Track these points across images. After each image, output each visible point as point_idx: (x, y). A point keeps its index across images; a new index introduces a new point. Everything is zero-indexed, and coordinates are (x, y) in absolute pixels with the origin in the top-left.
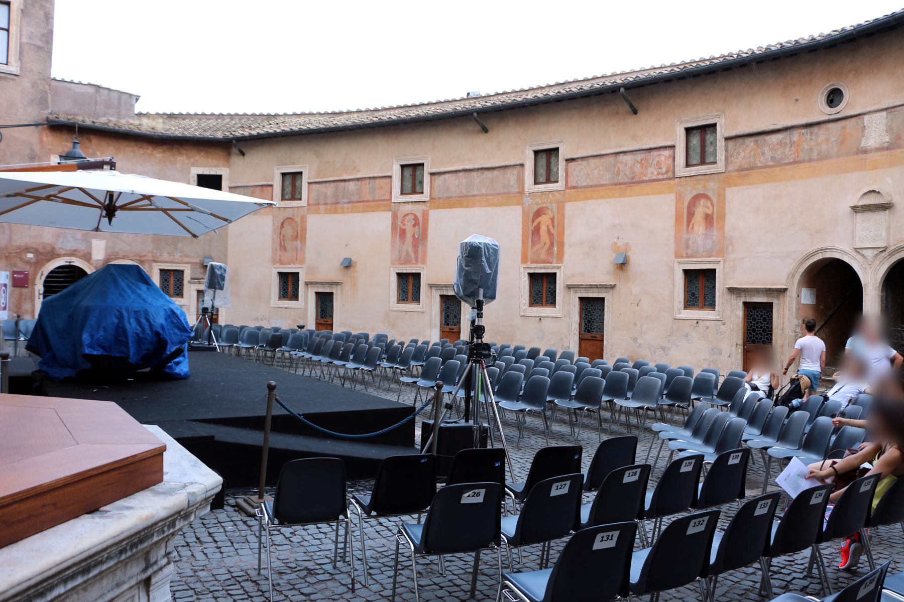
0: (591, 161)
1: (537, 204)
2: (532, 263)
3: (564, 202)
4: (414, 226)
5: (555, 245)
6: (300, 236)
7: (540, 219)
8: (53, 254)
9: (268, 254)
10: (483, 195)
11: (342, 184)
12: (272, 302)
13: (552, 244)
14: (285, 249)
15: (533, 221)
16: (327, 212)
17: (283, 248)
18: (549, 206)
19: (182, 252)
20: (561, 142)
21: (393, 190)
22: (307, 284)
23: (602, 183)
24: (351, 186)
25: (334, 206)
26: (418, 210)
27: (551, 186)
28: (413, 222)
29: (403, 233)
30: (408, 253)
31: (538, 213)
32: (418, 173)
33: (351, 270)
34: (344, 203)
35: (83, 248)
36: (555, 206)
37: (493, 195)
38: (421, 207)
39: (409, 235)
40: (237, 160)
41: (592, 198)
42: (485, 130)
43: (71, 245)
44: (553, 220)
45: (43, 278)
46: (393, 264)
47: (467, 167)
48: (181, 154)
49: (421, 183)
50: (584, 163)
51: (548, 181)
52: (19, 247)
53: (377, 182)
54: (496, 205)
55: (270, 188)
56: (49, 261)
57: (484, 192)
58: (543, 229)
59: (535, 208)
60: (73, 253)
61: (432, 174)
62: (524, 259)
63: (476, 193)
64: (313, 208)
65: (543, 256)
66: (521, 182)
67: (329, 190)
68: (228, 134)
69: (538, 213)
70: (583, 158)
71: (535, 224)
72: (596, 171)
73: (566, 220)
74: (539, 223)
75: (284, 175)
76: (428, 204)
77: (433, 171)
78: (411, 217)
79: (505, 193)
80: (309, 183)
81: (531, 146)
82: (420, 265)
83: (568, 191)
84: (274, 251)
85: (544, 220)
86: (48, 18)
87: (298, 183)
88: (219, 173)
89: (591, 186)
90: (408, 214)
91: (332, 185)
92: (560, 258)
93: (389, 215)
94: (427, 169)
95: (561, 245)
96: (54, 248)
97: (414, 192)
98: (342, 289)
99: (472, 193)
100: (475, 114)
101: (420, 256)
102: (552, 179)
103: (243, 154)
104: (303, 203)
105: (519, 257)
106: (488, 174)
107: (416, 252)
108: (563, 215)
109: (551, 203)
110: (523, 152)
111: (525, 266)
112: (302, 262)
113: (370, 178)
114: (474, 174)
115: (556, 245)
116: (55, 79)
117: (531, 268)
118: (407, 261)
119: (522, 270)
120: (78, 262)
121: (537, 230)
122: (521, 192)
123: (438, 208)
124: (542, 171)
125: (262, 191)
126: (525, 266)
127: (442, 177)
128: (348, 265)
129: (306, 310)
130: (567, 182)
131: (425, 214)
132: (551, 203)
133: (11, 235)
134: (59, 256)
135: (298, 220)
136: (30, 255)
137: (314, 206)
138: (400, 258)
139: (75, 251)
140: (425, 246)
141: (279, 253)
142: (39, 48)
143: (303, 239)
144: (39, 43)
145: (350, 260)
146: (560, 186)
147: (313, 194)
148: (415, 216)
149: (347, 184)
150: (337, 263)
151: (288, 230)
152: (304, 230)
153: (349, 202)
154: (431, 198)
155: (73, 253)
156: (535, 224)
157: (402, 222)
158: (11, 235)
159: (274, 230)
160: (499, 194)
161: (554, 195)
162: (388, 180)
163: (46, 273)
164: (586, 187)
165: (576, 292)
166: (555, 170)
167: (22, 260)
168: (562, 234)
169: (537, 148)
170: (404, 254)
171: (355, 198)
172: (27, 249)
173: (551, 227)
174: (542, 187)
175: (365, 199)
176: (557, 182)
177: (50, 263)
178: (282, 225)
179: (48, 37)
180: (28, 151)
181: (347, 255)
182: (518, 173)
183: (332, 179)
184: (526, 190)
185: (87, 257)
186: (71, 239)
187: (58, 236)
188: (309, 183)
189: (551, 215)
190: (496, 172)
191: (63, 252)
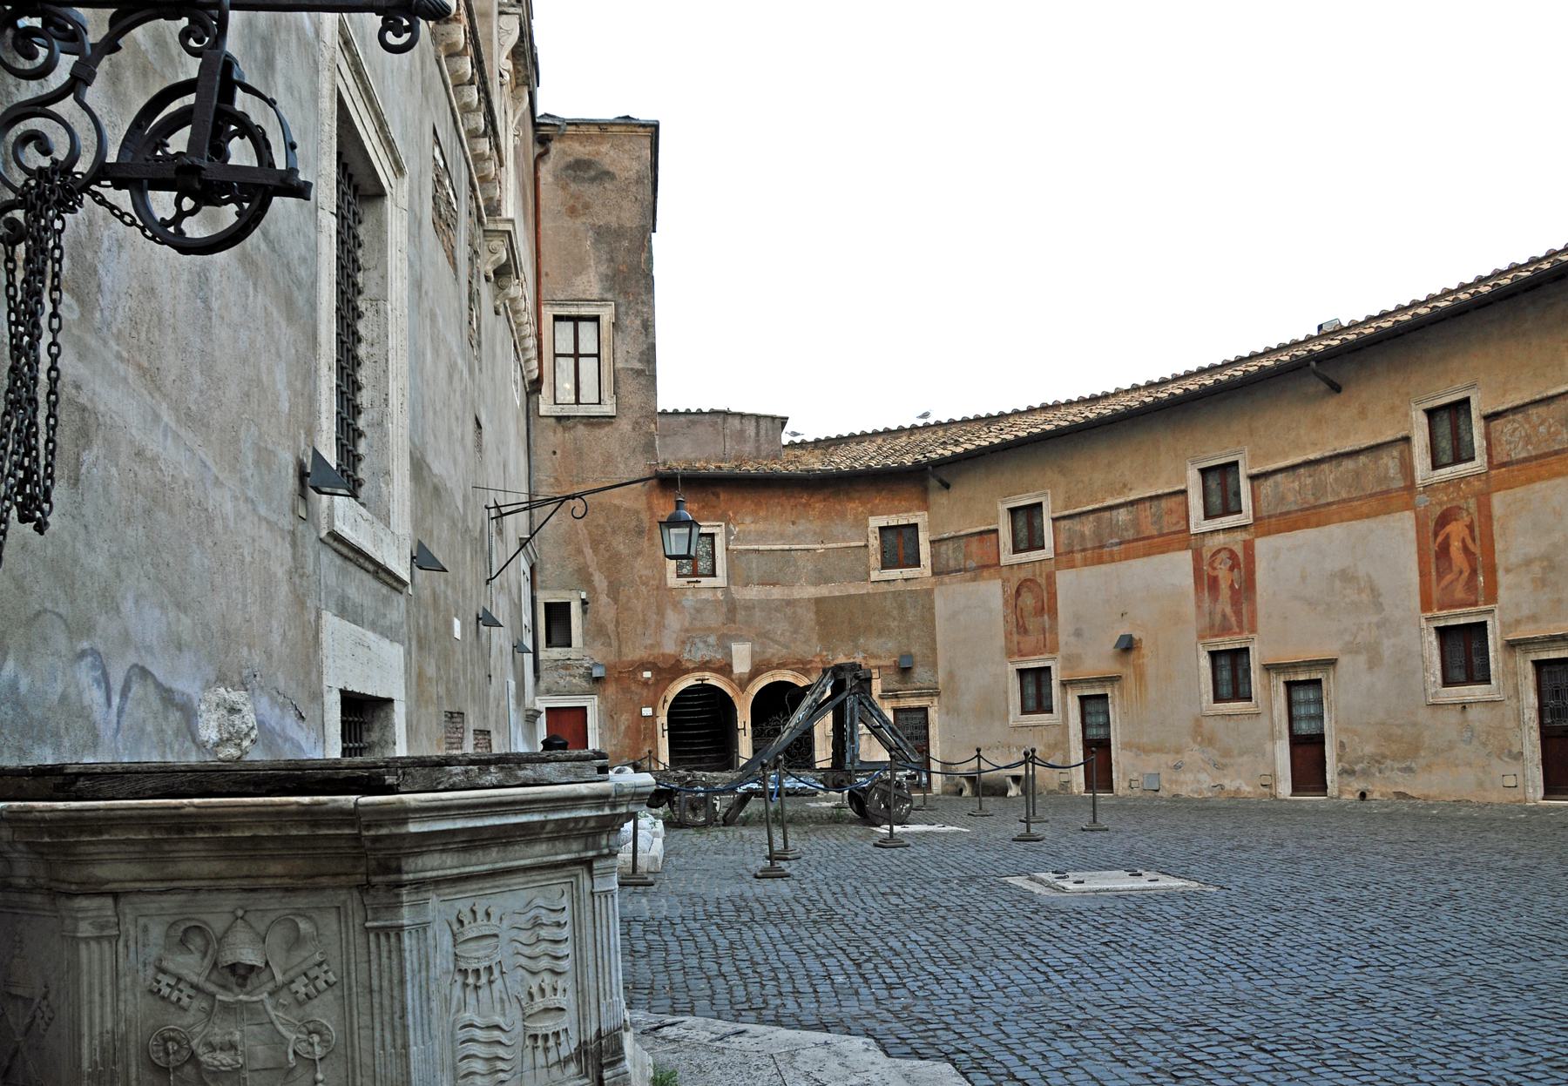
0: (1533, 411)
1: (1440, 504)
2: (1440, 609)
3: (1489, 494)
4: (1231, 569)
5: (1480, 571)
6: (1048, 607)
7: (1448, 529)
8: (676, 669)
9: (1000, 641)
10: (1344, 501)
11: (1107, 514)
12: (1011, 718)
13: (1474, 572)
14: (1026, 631)
15: (1436, 535)
16: (1085, 564)
17: (1022, 629)
18: (1462, 503)
19: (865, 651)
20: (1473, 386)
21: (1192, 514)
22: (1064, 684)
23: (1557, 447)
24: (1122, 515)
25: (1098, 554)
26: (1236, 541)
27: (1462, 469)
28: (1230, 563)
29: (1214, 583)
30: (1224, 616)
31: (1444, 519)
32: (1230, 479)
33: (1133, 655)
34: (1113, 545)
36: (1472, 503)
37: (1360, 498)
38: (1241, 536)
39: (1224, 586)
40: (940, 499)
41: (1540, 478)
42: (1336, 388)
43: (701, 653)
44: (1471, 527)
45: (667, 706)
46: (1201, 637)
47: (1312, 457)
48: (851, 499)
49: (1237, 494)
50: (1519, 417)
51: (1457, 460)
52: (632, 663)
53: (1164, 504)
54: (1368, 517)
55: (993, 536)
57: (1344, 495)
58: (1455, 545)
59: (1438, 511)
60: (704, 666)
61: (1253, 478)
62: (1426, 605)
63: (1330, 499)
64: (1064, 559)
65: (1459, 594)
66: (1407, 468)
67: (1087, 527)
68: (920, 457)
69: (1444, 519)
70: (1515, 410)
71: (1439, 539)
72: (1542, 429)
73: (1496, 527)
74: (1447, 537)
75: (1013, 511)
76: (1252, 529)
77: (1255, 471)
78: (1224, 555)
79: (1382, 493)
80: (1054, 520)
81: (1418, 403)
82: (1246, 634)
83: (1493, 472)
84: (1008, 635)
85: (1456, 530)
86: (648, 327)
87: (1036, 523)
88: (912, 521)
89: (1537, 457)
90: (1219, 551)
91: (1091, 518)
92: (1492, 596)
93: (1188, 555)
94: (1243, 471)
95: (1491, 571)
97: (1227, 512)
98: (1121, 689)
99: (1323, 501)
100: (1313, 364)
101: (1245, 620)
102: (1464, 455)
103: (947, 486)
104: (1048, 552)
105: (1416, 601)
106: (1349, 464)
107: (1238, 613)
108: (1490, 517)
109: (1466, 498)
110: (1407, 415)
111: (1429, 615)
112: (1054, 649)
113: (1151, 498)
114: (1325, 467)
115: (1482, 573)
116: (664, 413)
117: (1438, 618)
118: (1225, 630)
119: (1424, 624)
120: (713, 680)
121: (1444, 551)
122: (1410, 487)
123: (1269, 533)
124: (1445, 444)
125: (981, 541)
126: (1429, 615)
127: (1270, 481)
128: (1127, 646)
129: (1065, 727)
130: (1490, 456)
131: (1249, 547)
132: (1466, 498)
134: (687, 671)
135: (1042, 581)
136: (647, 674)
137: (1065, 557)
138: (1212, 627)
140: (1251, 599)
141: (1016, 638)
142: (639, 373)
143: (1053, 612)
144: (638, 366)
145: (1130, 637)
146: (1479, 463)
147: (1063, 538)
148: (1232, 552)
149: (1114, 513)
150: (1109, 644)
151: (1028, 600)
152: (1053, 596)
153: (1120, 543)
154: (1256, 519)
155: (704, 666)
156: (1439, 539)
157: (1211, 564)
159: (1006, 603)
160: (1371, 495)
161: (1468, 483)
162: (1180, 498)
163: (670, 699)
164: (1525, 460)
165: (1527, 652)
166: (1467, 438)
167: (636, 681)
168: (1490, 550)
169: (1429, 405)
170: (1218, 618)
171: (1130, 534)
172: (644, 666)
173: (1469, 541)
174: (1445, 473)
175: (1147, 534)
176: (1473, 459)
178: (1018, 592)
179: (649, 355)
180: (634, 523)
181: (1125, 631)
182: (1401, 453)
183: (1090, 508)
184: (1418, 481)
185: (725, 669)
186: (701, 645)
187: (684, 642)
188: (1054, 520)
189: (1467, 520)
190: (1362, 459)
191: (691, 666)
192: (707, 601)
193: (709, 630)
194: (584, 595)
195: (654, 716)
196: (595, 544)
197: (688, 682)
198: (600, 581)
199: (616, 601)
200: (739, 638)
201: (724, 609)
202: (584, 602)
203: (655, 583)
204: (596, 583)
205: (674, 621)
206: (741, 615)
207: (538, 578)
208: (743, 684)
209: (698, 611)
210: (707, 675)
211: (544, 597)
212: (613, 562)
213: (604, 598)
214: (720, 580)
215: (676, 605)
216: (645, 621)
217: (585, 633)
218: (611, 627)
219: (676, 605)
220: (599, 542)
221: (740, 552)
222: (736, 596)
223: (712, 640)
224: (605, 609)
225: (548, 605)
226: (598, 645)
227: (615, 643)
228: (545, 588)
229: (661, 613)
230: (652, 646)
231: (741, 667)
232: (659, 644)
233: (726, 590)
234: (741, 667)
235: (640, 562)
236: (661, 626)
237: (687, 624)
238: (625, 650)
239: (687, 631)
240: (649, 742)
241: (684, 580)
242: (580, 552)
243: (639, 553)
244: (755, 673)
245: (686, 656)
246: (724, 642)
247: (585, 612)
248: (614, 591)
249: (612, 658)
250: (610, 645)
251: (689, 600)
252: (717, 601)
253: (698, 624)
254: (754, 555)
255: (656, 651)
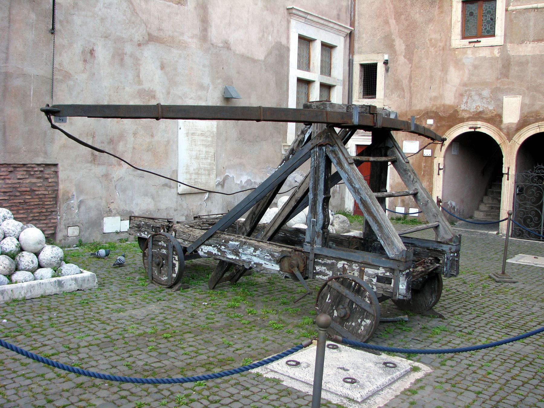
8: (454, 118)
35: (491, 108)
43: (475, 104)
56: (450, 127)
96: (456, 111)
120: (485, 128)
133: (411, 98)
139: (481, 112)
155: (478, 116)
158: (411, 98)
172: (428, 114)
177: (452, 129)
185: (496, 119)
186: (476, 98)
187: (462, 95)
191: (466, 115)
192: (485, 58)
193: (485, 84)
194: (386, 57)
195: (432, 157)
196: (398, 15)
197: (463, 129)
198: (400, 45)
199: (410, 60)
200: (510, 91)
201: (500, 66)
202: (386, 63)
203: (441, 44)
204: (397, 47)
205: (455, 77)
206: (514, 70)
207: (356, 46)
208: (510, 135)
209: (476, 67)
210: (479, 124)
211: (359, 59)
212: (411, 30)
213: (402, 59)
214: (498, 39)
215: (458, 63)
216: (431, 77)
217: (386, 86)
218: (405, 82)
219: (458, 63)
220: (401, 14)
221: (520, 12)
222: (511, 53)
223: (486, 93)
224: (402, 67)
225: (362, 65)
226: (395, 96)
227: (407, 95)
228: (360, 53)
229: (445, 70)
230: (436, 98)
231: (511, 115)
232: (441, 96)
233: (503, 48)
234: (511, 115)
235: (431, 27)
236: (444, 81)
237: (465, 79)
238: (415, 101)
239: (465, 85)
240: (426, 179)
241: (466, 41)
242: (387, 22)
243: (431, 20)
244: (523, 123)
245: (463, 107)
246: (497, 94)
247: (387, 70)
248: (410, 53)
249: (404, 108)
250: (404, 97)
251: (469, 58)
252: (493, 58)
253: (475, 79)
254: (532, 14)
255: (438, 103)
